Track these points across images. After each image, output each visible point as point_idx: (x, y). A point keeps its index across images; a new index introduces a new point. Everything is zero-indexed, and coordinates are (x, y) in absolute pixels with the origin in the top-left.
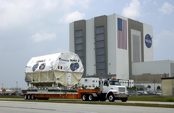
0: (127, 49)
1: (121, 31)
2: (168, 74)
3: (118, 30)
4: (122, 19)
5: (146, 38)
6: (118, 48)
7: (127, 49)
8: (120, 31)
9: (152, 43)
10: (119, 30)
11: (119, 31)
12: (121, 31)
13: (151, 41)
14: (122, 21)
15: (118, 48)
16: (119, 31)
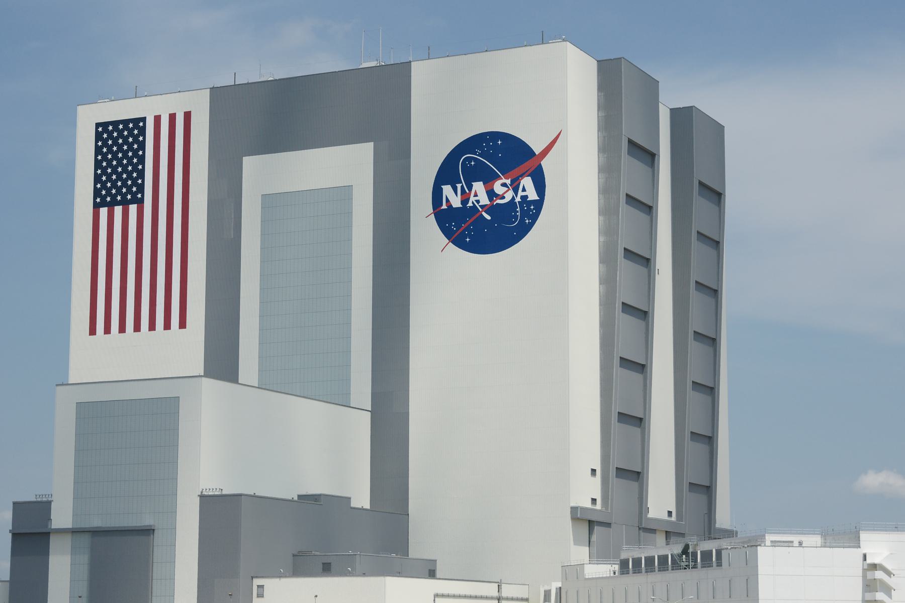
0: (183, 324)
1: (133, 208)
2: (43, 508)
3: (96, 207)
4: (144, 119)
5: (447, 173)
6: (93, 331)
7: (183, 324)
8: (118, 210)
9: (539, 204)
10: (111, 206)
11: (104, 211)
12: (133, 208)
13: (527, 182)
14: (143, 132)
15: (93, 331)
16: (104, 211)
